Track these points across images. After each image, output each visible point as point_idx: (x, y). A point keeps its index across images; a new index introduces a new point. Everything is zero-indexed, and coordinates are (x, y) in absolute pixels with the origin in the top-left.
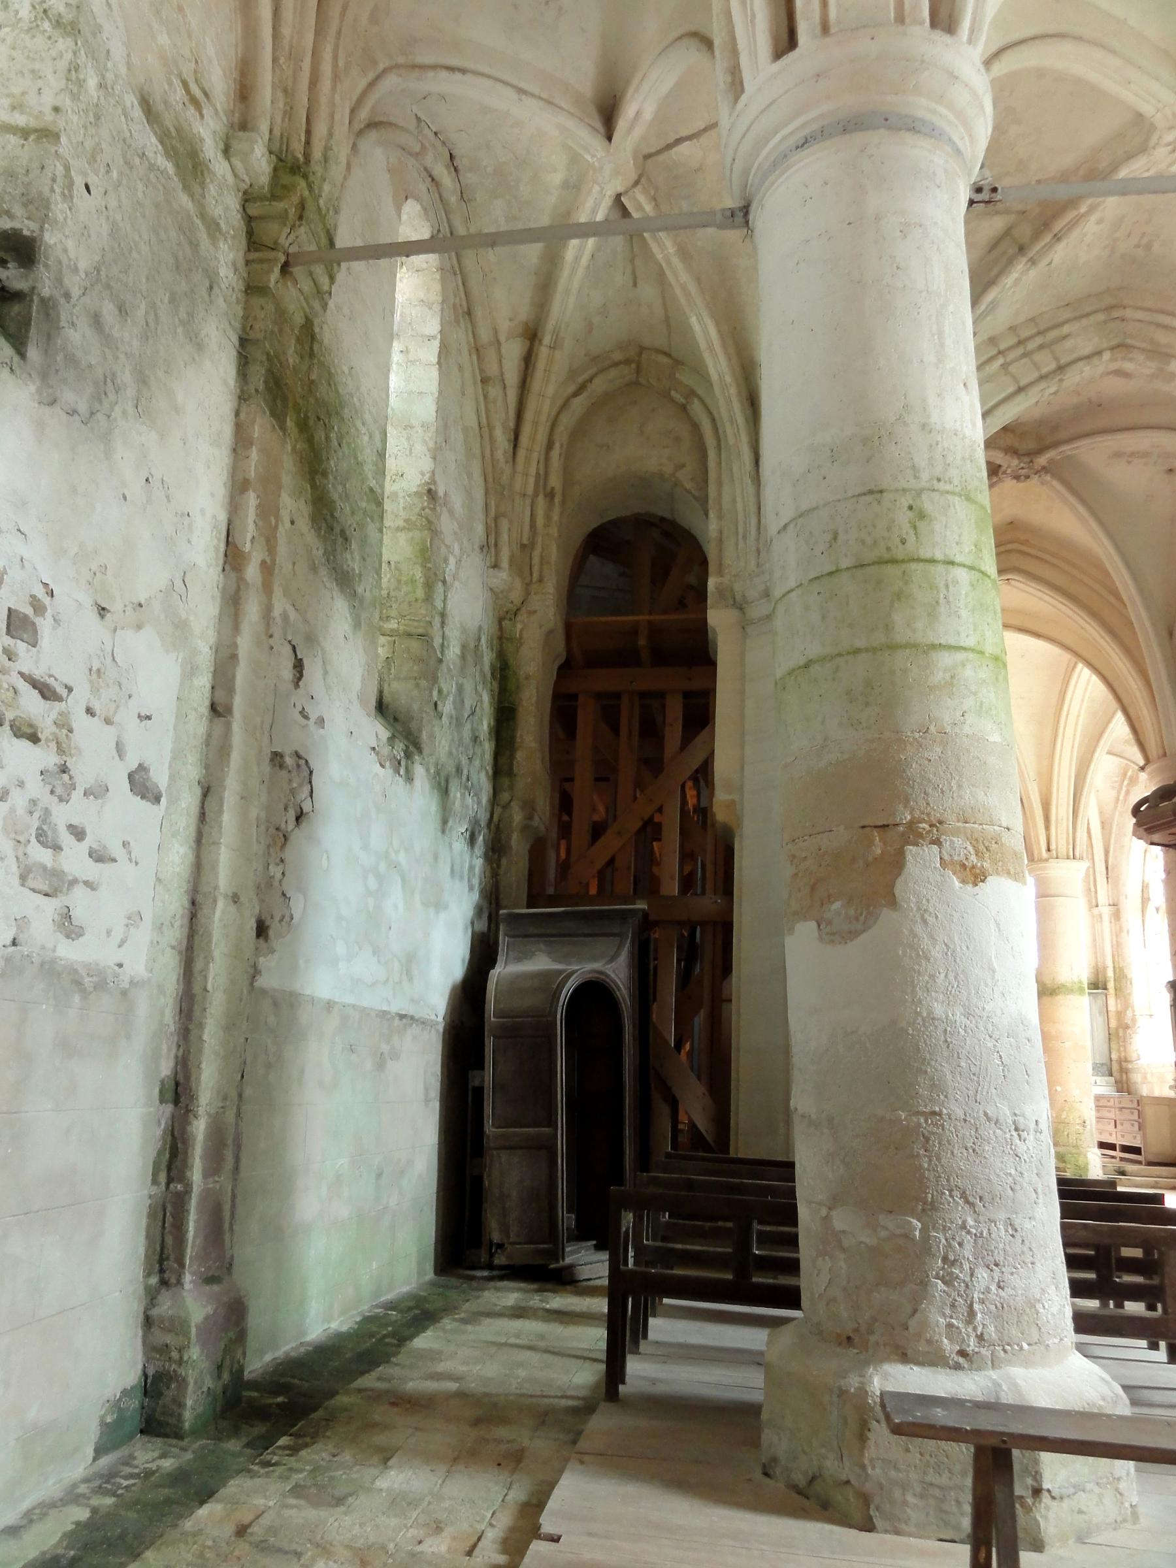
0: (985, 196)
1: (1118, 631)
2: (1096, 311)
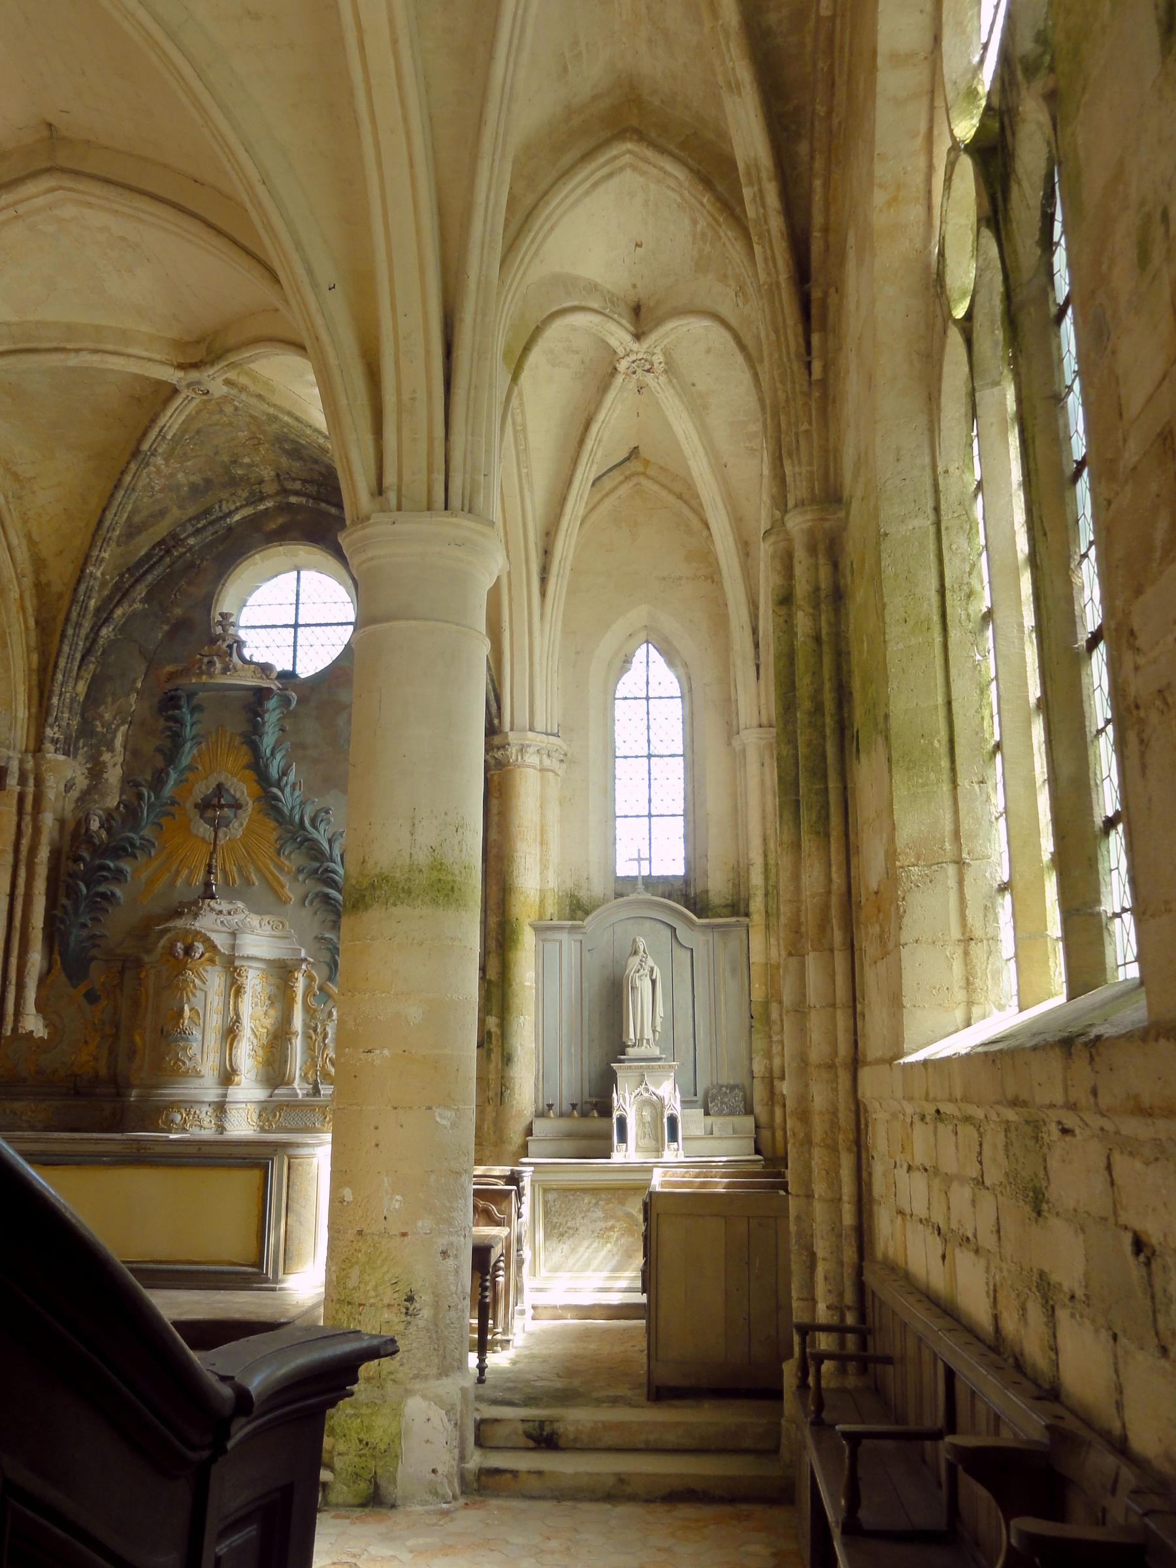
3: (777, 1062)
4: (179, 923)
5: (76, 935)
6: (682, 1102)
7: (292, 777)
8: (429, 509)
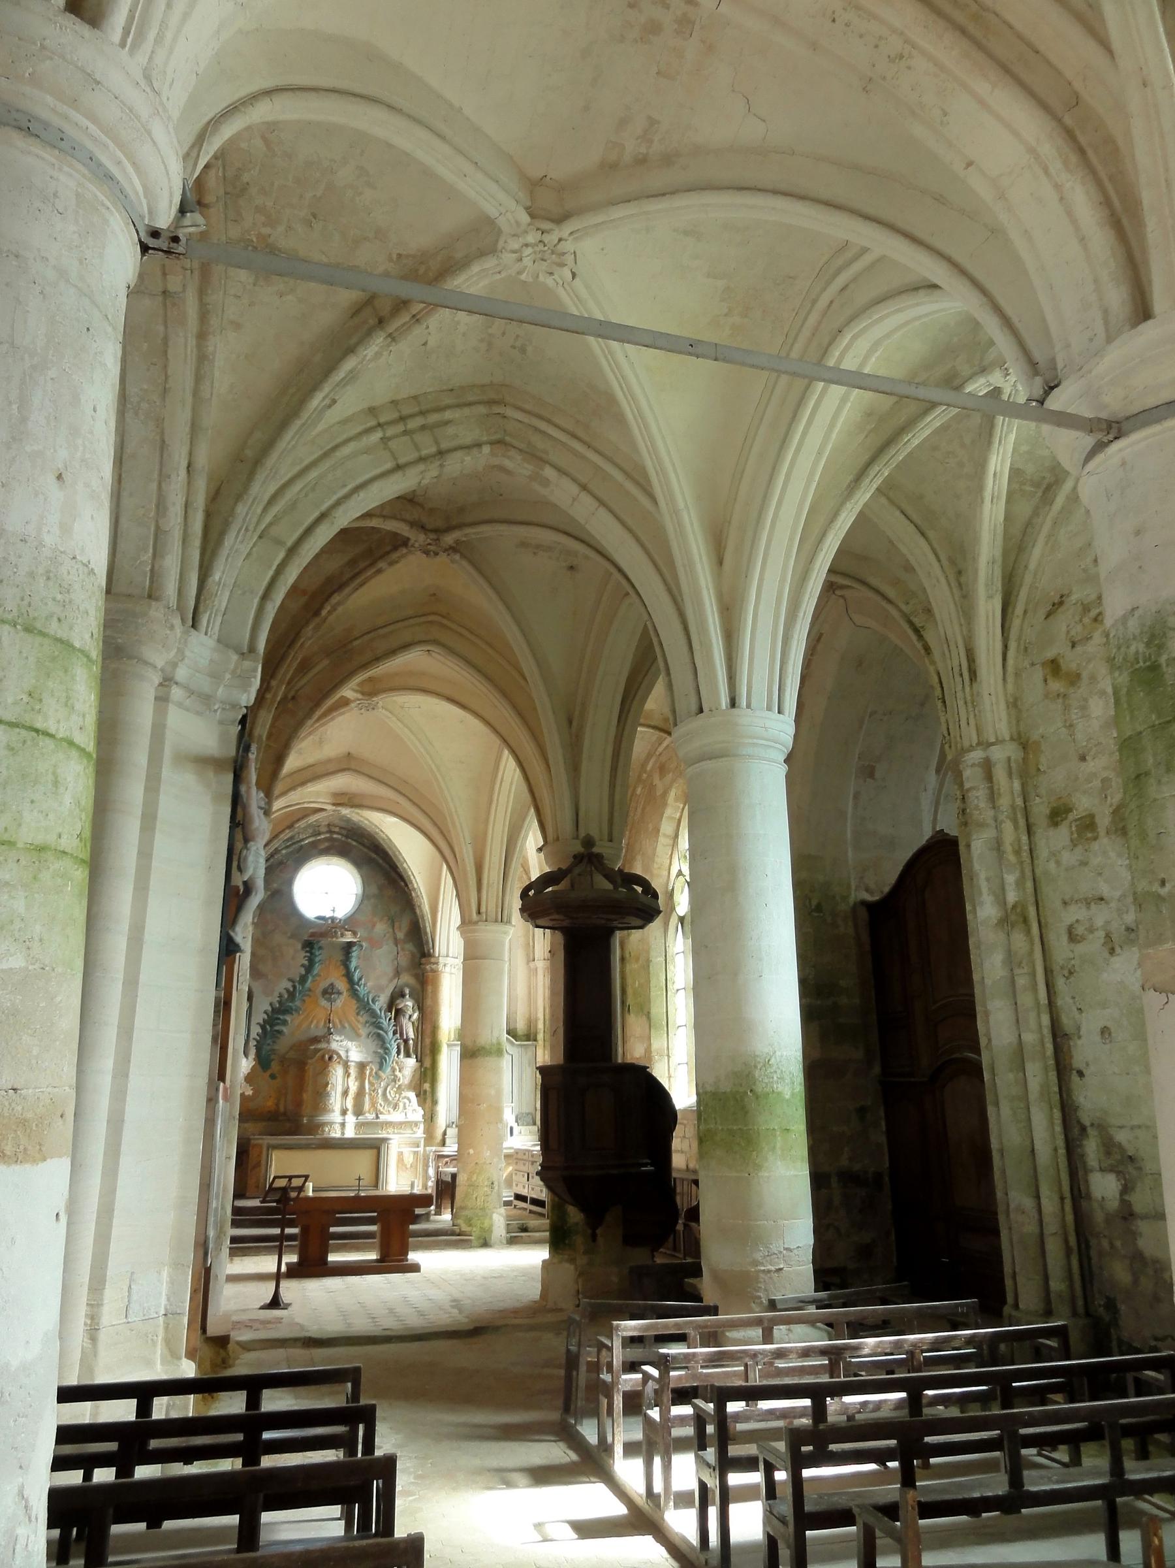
0: (162, 243)
1: (525, 716)
2: (479, 403)
4: (323, 1045)
5: (266, 1048)
7: (363, 981)
8: (496, 921)
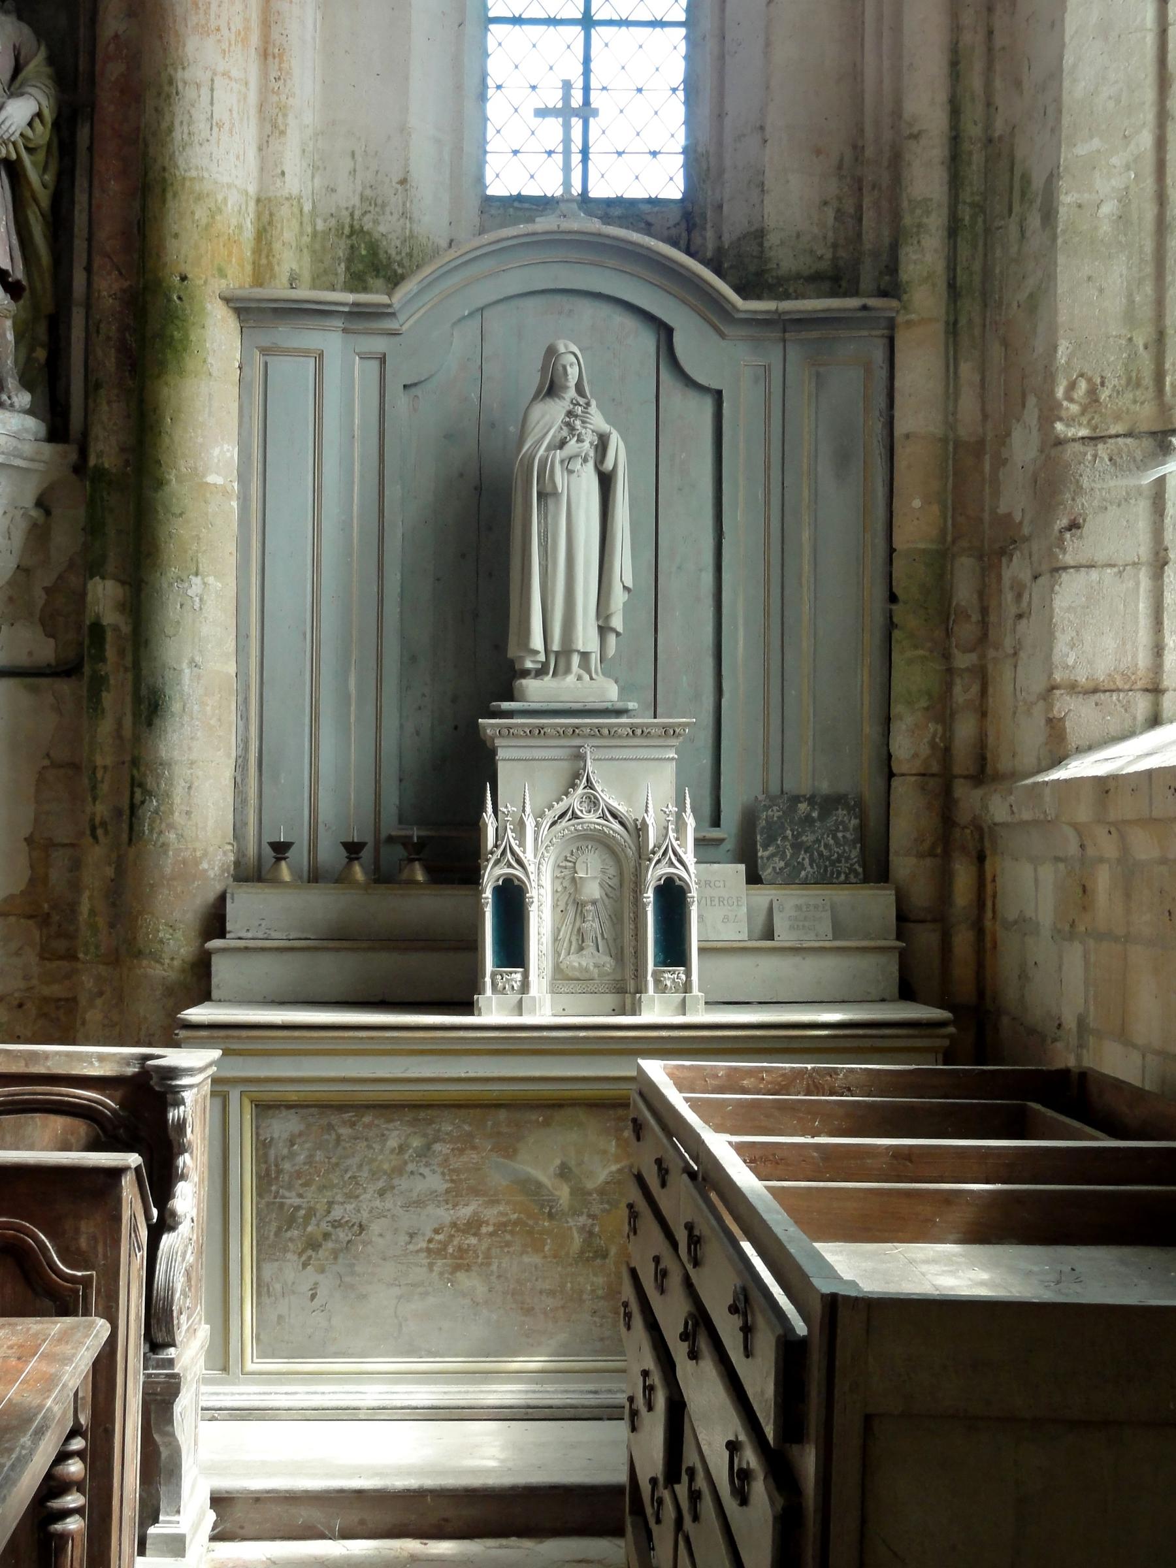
3: (965, 730)
6: (700, 842)
